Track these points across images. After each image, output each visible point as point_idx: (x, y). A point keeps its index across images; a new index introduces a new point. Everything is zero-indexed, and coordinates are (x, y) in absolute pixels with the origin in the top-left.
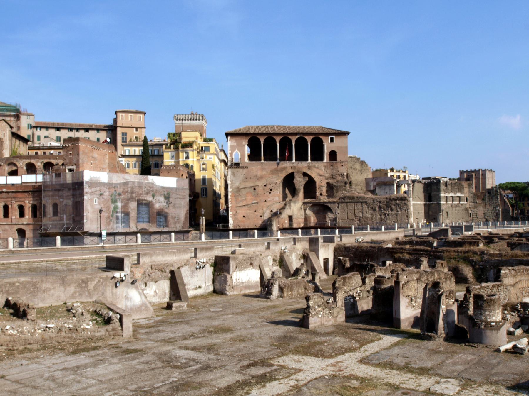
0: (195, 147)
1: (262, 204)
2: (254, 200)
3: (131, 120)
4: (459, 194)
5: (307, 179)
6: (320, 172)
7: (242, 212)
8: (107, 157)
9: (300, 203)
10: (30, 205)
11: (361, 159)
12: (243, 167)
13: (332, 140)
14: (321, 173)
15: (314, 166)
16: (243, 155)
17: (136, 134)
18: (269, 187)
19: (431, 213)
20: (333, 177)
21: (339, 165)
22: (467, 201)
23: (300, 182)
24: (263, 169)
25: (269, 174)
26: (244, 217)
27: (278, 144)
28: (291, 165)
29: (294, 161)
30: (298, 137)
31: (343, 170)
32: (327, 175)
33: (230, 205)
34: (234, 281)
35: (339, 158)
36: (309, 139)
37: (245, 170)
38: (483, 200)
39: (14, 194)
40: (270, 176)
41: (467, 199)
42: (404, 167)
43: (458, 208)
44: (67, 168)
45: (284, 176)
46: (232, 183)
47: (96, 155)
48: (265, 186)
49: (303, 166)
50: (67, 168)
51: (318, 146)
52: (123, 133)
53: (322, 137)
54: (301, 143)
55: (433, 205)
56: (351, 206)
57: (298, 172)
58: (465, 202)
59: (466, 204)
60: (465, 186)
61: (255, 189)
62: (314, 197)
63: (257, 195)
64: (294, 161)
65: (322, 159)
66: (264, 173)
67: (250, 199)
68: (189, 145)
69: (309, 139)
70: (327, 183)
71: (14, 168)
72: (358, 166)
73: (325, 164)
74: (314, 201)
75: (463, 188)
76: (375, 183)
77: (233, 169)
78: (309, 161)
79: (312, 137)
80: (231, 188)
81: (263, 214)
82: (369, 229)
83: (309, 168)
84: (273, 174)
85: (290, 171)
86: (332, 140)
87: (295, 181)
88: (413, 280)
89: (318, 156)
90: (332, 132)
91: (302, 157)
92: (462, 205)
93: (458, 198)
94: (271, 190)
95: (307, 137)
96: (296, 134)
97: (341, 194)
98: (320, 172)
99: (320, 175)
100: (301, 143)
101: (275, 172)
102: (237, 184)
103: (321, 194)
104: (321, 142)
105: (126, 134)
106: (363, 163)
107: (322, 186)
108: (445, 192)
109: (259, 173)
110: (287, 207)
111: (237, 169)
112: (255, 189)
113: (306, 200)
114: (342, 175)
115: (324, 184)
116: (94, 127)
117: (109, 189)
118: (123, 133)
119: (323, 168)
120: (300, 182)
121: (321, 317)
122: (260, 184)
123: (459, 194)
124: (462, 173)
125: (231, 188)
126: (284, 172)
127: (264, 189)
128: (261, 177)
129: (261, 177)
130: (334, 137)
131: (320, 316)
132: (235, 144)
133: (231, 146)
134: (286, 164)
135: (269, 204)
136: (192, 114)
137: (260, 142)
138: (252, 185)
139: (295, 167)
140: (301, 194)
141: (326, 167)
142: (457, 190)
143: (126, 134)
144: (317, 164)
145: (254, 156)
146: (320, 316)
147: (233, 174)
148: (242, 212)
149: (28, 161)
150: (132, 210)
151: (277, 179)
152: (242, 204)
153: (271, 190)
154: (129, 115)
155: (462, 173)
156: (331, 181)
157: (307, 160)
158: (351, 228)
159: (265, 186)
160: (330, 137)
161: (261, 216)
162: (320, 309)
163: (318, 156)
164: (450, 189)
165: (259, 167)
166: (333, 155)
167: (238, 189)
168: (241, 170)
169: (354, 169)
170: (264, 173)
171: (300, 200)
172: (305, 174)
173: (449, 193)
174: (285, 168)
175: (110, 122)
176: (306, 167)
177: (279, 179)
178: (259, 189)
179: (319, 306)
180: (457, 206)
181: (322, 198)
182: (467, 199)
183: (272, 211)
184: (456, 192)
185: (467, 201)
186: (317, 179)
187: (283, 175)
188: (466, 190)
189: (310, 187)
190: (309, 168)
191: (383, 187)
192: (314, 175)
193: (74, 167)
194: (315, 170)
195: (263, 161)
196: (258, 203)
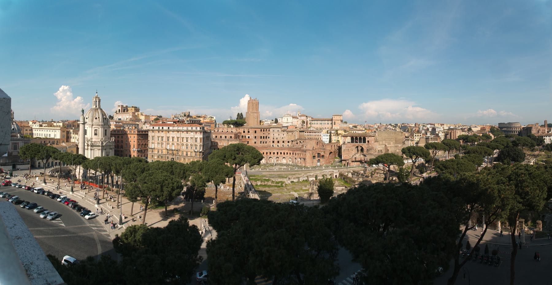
6: (365, 146)
7: (345, 156)
23: (360, 148)
31: (371, 146)
49: (361, 144)
54: (360, 138)
67: (347, 152)
89: (364, 142)
91: (360, 142)
97: (370, 152)
98: (365, 146)
100: (360, 138)
148: (345, 156)
163: (364, 142)
166: (368, 141)
189: (362, 150)
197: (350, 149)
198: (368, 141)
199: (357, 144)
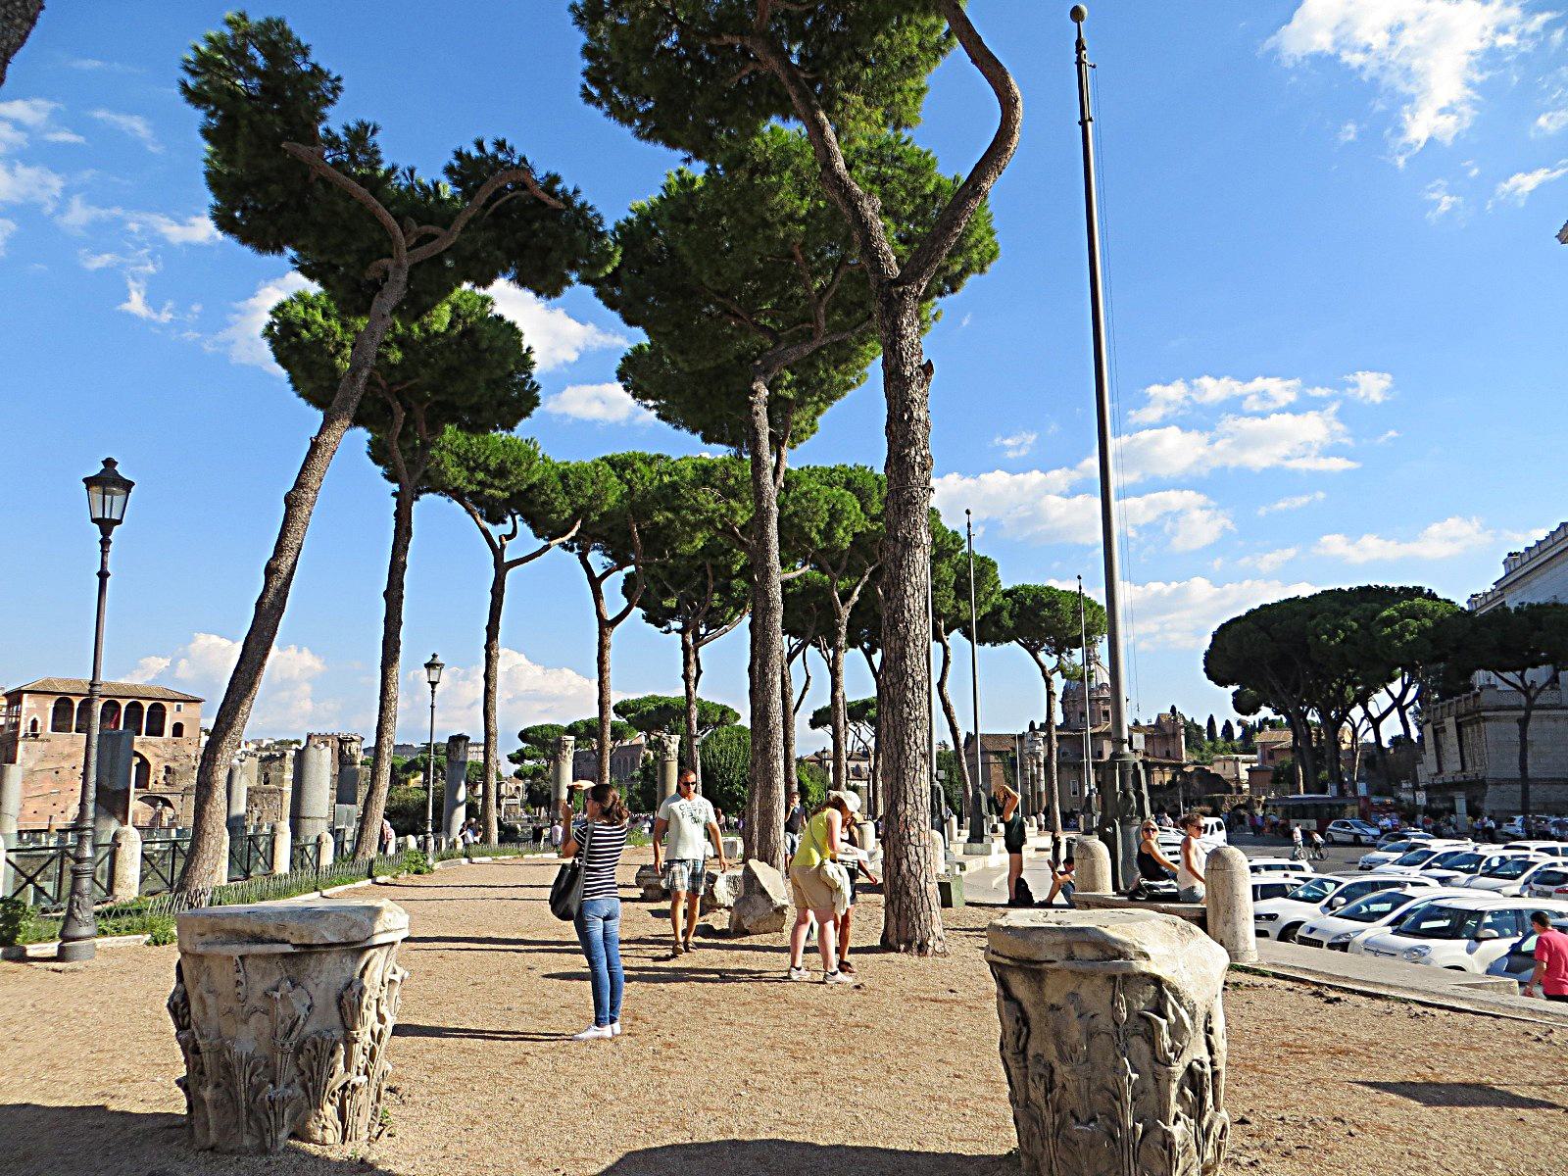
15: (150, 743)
16: (45, 723)
36: (146, 705)
51: (158, 713)
54: (135, 708)
65: (160, 733)
69: (146, 705)
83: (143, 745)
89: (156, 730)
95: (142, 702)
100: (135, 708)
102: (31, 764)
104: (163, 708)
128: (69, 756)
145: (60, 723)
156: (172, 765)
166: (178, 730)
190: (143, 745)
192: (147, 756)
198: (178, 730)
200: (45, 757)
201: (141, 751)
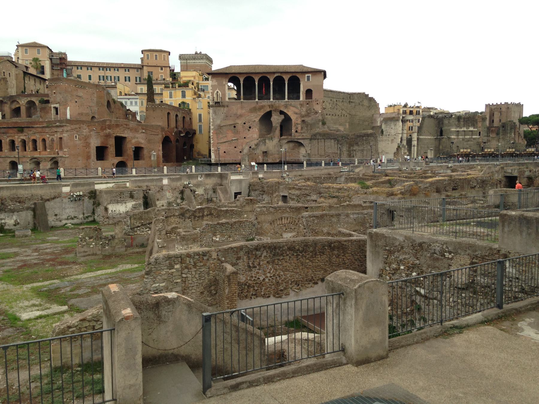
0: (190, 86)
1: (242, 141)
2: (235, 137)
3: (156, 59)
4: (471, 129)
5: (283, 117)
8: (95, 96)
9: (276, 140)
10: (20, 140)
11: (370, 96)
12: (224, 106)
13: (308, 77)
14: (297, 111)
15: (291, 105)
17: (161, 73)
18: (248, 125)
19: (441, 147)
20: (308, 115)
21: (314, 103)
22: (479, 135)
23: (277, 119)
24: (242, 108)
25: (250, 112)
26: (225, 152)
27: (257, 84)
28: (269, 104)
29: (272, 100)
30: (246, 76)
32: (303, 113)
33: (212, 142)
34: (110, 212)
35: (315, 95)
36: (286, 78)
37: (226, 109)
38: (498, 134)
39: (40, 130)
40: (249, 114)
41: (480, 133)
42: (419, 103)
43: (469, 143)
44: (53, 106)
45: (262, 114)
46: (213, 121)
47: (81, 94)
48: (245, 123)
49: (281, 104)
50: (53, 106)
52: (149, 72)
53: (298, 76)
55: (444, 140)
56: (322, 143)
57: (275, 110)
58: (478, 137)
59: (479, 138)
60: (478, 121)
61: (235, 127)
62: (291, 135)
63: (237, 132)
64: (286, 100)
65: (298, 98)
66: (244, 111)
67: (230, 136)
68: (186, 85)
69: (286, 78)
70: (303, 121)
71: (17, 106)
72: (366, 103)
73: (302, 103)
74: (290, 137)
75: (477, 123)
76: (382, 119)
77: (215, 108)
78: (286, 100)
79: (289, 76)
80: (212, 125)
81: (243, 150)
82: (323, 165)
83: (286, 106)
84: (252, 112)
85: (268, 110)
86: (308, 77)
87: (272, 119)
88: (174, 215)
90: (309, 70)
92: (474, 139)
93: (471, 133)
94: (250, 128)
95: (284, 77)
96: (274, 73)
99: (296, 114)
100: (279, 81)
101: (254, 110)
102: (218, 122)
103: (296, 132)
105: (152, 72)
106: (372, 100)
107: (297, 124)
108: (458, 126)
109: (239, 112)
110: (261, 143)
111: (218, 108)
112: (235, 127)
113: (283, 137)
114: (316, 113)
115: (299, 121)
116: (122, 66)
117: (88, 126)
118: (149, 72)
119: (299, 107)
120: (277, 119)
121: (93, 248)
122: (240, 122)
123: (471, 129)
124: (487, 106)
125: (212, 125)
126: (262, 110)
127: (243, 127)
128: (241, 116)
129: (241, 116)
130: (310, 75)
131: (92, 246)
132: (216, 83)
133: (212, 86)
134: (265, 103)
135: (248, 141)
136: (196, 53)
137: (240, 81)
138: (231, 122)
139: (272, 106)
140: (278, 132)
141: (302, 105)
142: (470, 124)
143: (152, 72)
144: (293, 102)
146: (92, 246)
147: (215, 112)
148: (223, 148)
149: (29, 99)
150: (110, 145)
151: (256, 118)
152: (223, 140)
153: (250, 128)
154: (155, 54)
155: (487, 106)
156: (306, 119)
157: (285, 99)
158: (303, 163)
159: (245, 123)
160: (306, 75)
161: (241, 152)
162: (92, 240)
164: (462, 123)
165: (239, 105)
166: (309, 93)
167: (220, 127)
168: (222, 109)
169: (363, 105)
170: (244, 111)
171: (276, 137)
172: (282, 113)
173: (461, 128)
174: (262, 107)
175: (139, 62)
176: (283, 105)
177: (256, 117)
178: (239, 127)
179: (90, 238)
180: (468, 140)
181: (297, 134)
182: (480, 133)
183: (250, 147)
184: (469, 126)
185: (479, 135)
186: (293, 117)
187: (262, 113)
188: (480, 124)
189: (286, 123)
190: (286, 106)
191: (389, 122)
192: (289, 114)
193: (57, 106)
194: (292, 108)
195: (242, 100)
196: (237, 140)
197: (240, 122)
198: (309, 93)
199: (267, 104)
200: (227, 117)
201: (285, 111)
